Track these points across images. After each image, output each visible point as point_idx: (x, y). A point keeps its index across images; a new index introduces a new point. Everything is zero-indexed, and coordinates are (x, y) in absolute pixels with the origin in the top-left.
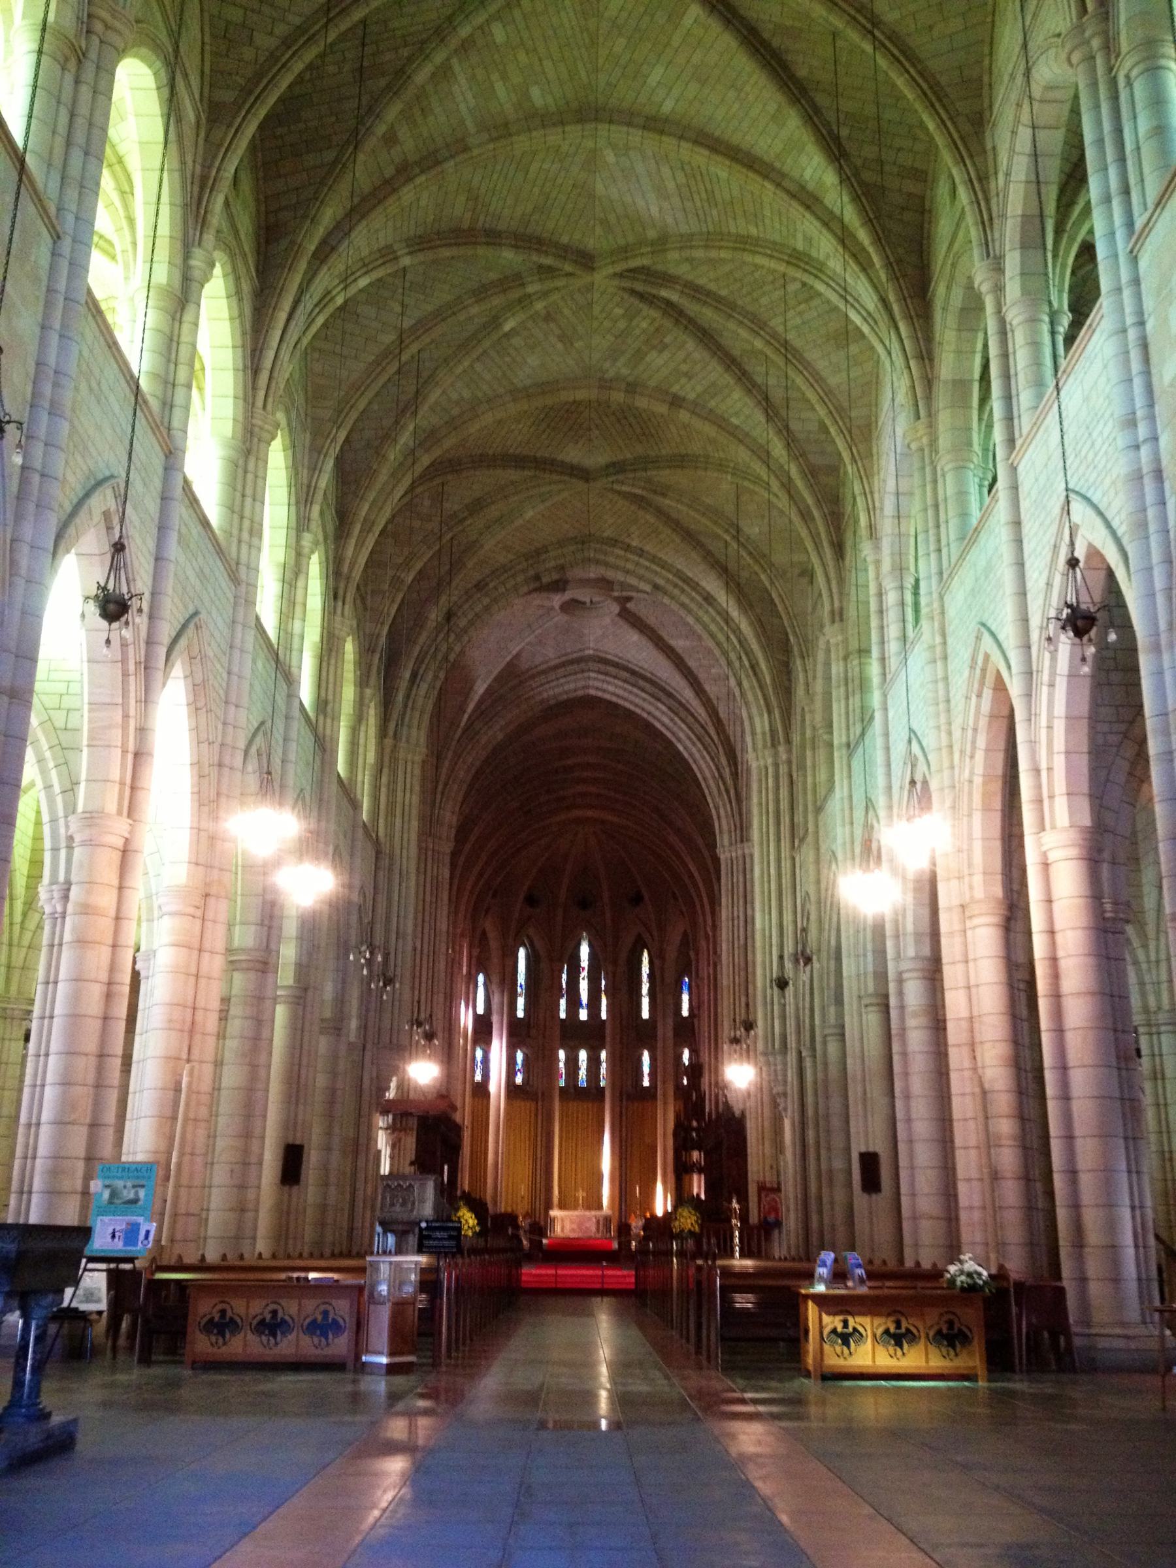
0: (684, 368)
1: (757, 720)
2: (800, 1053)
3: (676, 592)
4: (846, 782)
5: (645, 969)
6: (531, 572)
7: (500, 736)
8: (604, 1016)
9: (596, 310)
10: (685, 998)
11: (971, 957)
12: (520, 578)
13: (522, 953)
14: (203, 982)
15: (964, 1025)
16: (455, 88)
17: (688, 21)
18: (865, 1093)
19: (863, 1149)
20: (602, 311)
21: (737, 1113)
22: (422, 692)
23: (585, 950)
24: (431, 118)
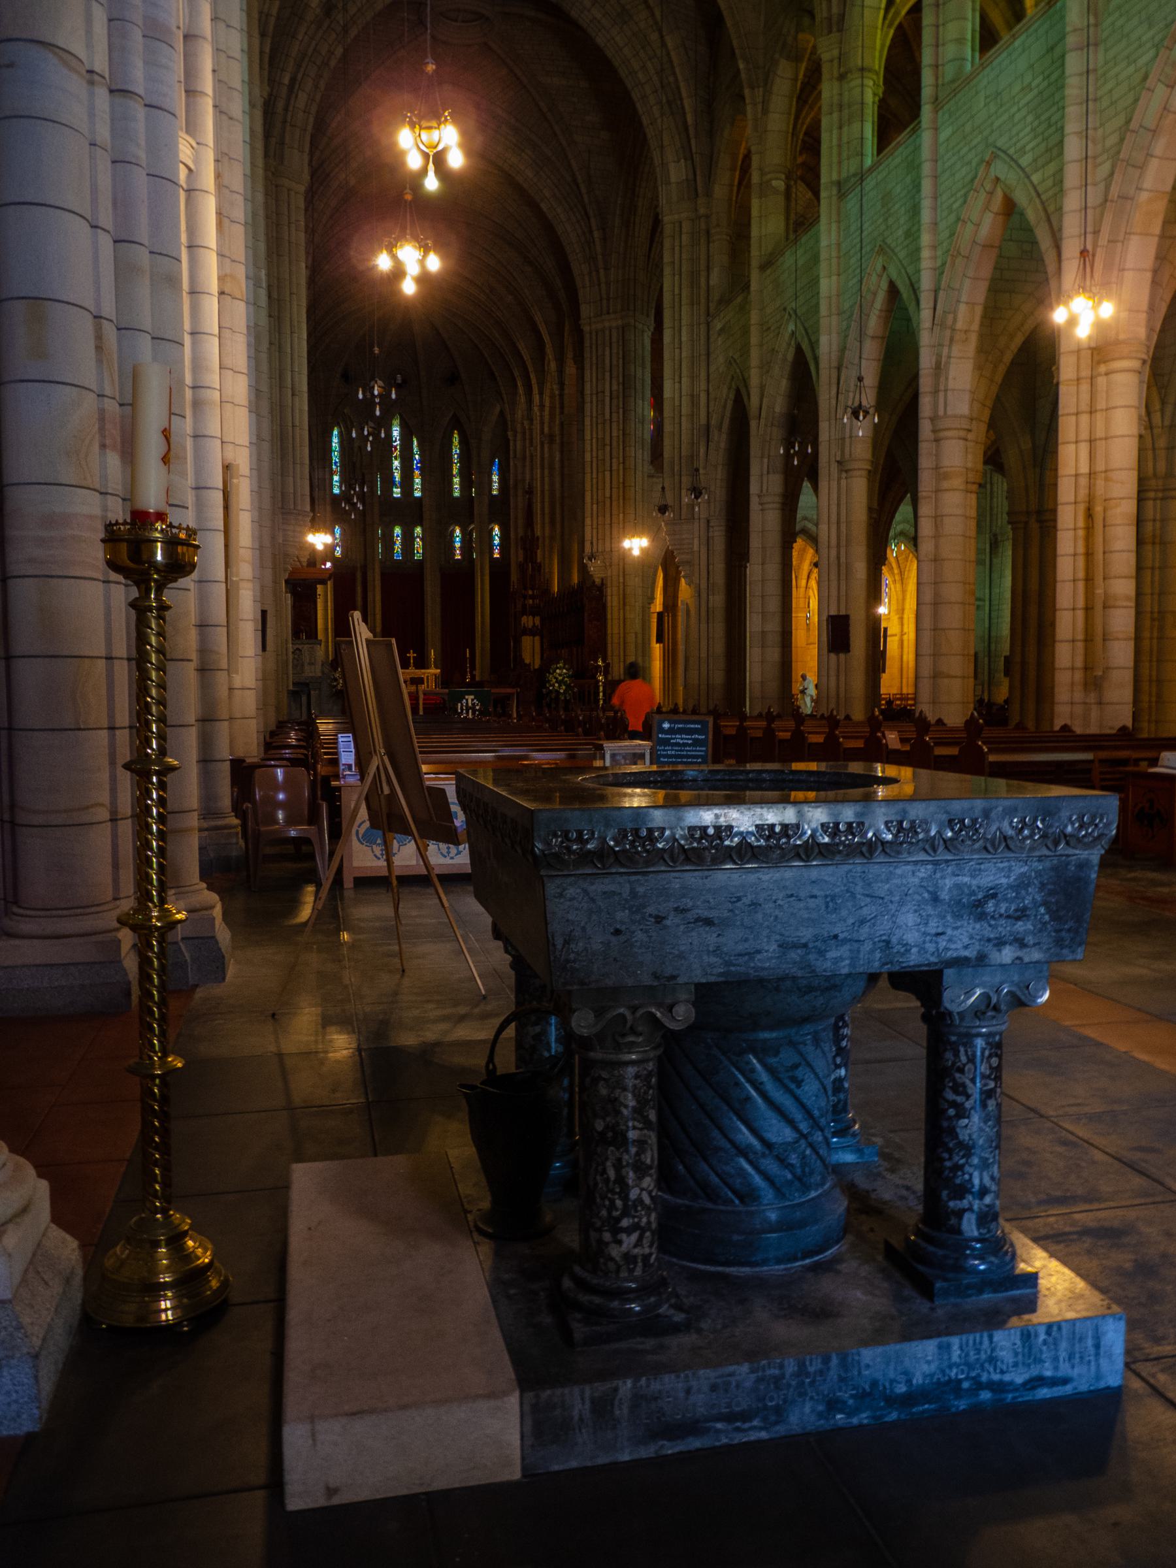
1: (672, 168)
2: (708, 521)
4: (834, 226)
5: (456, 451)
8: (418, 494)
10: (495, 478)
11: (1101, 404)
13: (335, 432)
14: (228, 406)
15: (1083, 481)
18: (838, 558)
19: (833, 612)
21: (598, 581)
23: (396, 432)
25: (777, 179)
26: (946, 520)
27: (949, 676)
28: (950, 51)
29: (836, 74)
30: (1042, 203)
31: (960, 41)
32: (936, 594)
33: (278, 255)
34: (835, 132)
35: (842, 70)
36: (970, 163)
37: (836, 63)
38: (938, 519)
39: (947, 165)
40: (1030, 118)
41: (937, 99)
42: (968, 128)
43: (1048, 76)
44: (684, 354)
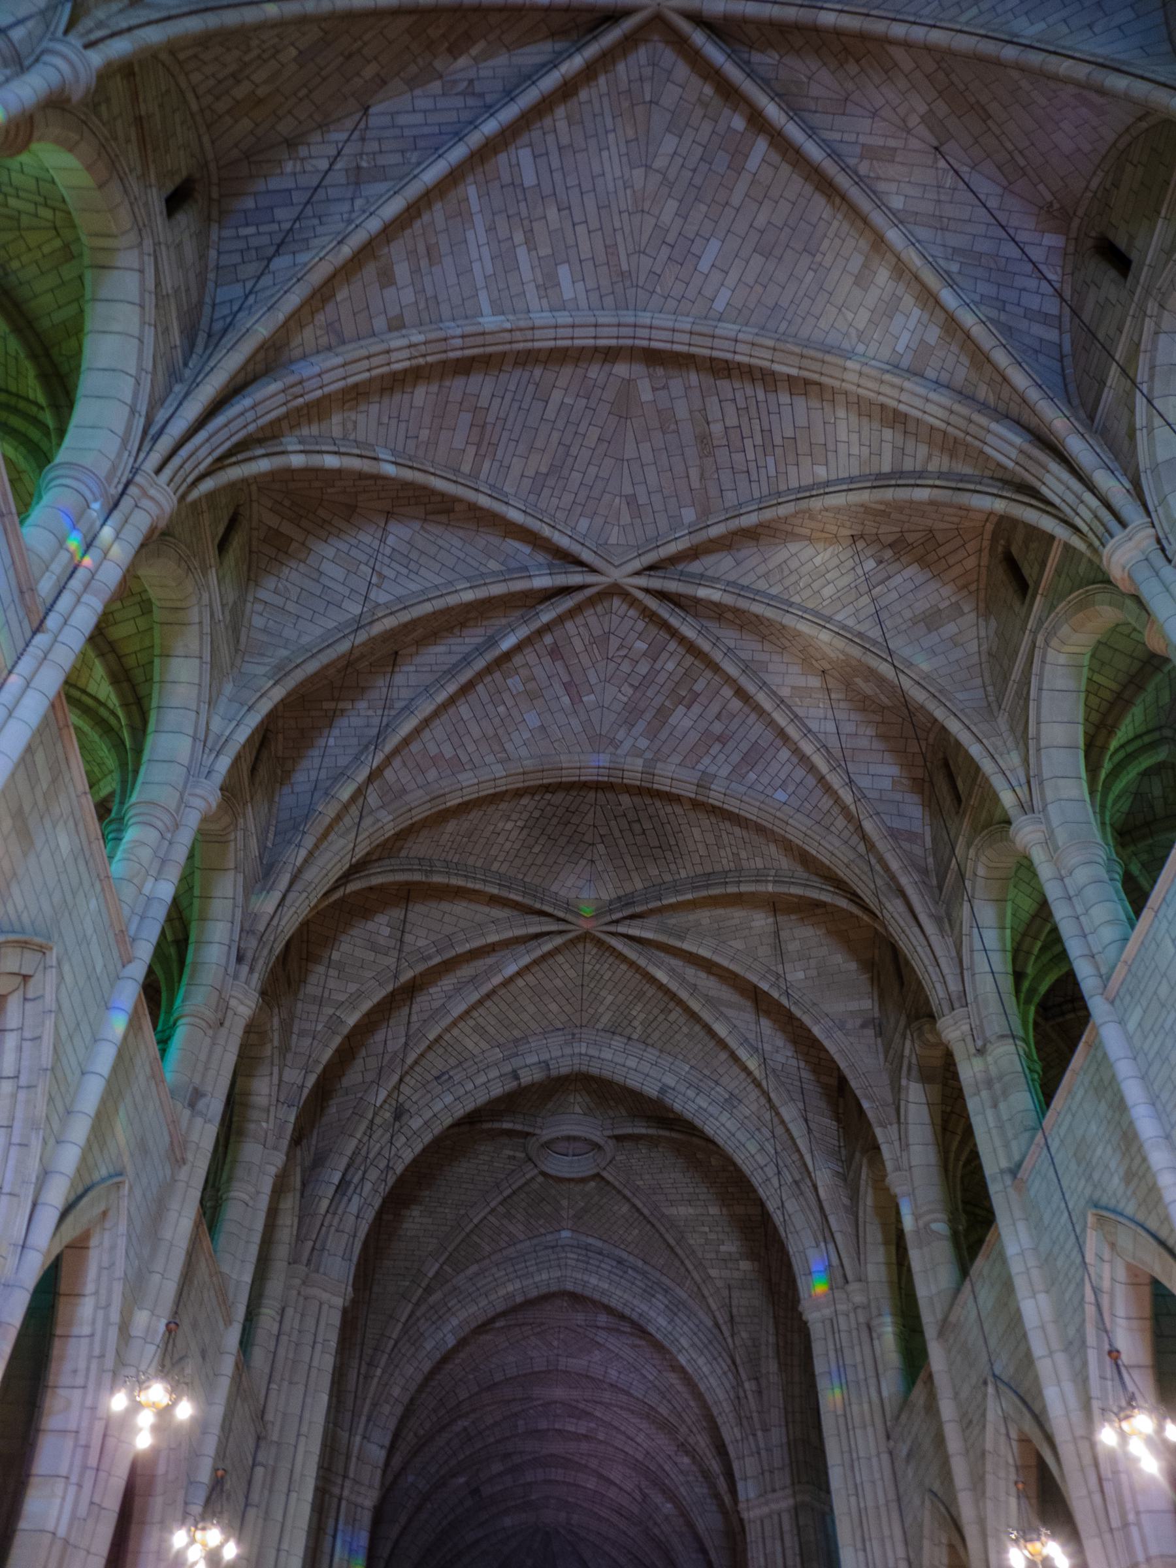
0: (717, 728)
3: (691, 1093)
4: (1021, 1226)
6: (507, 1069)
7: (451, 1341)
9: (614, 642)
12: (494, 1073)
16: (470, 235)
17: (753, 163)
20: (621, 647)
22: (353, 1208)
24: (436, 269)
25: (935, 1221)
29: (973, 1051)
33: (291, 1383)
34: (990, 1113)
35: (980, 1043)
37: (969, 1039)
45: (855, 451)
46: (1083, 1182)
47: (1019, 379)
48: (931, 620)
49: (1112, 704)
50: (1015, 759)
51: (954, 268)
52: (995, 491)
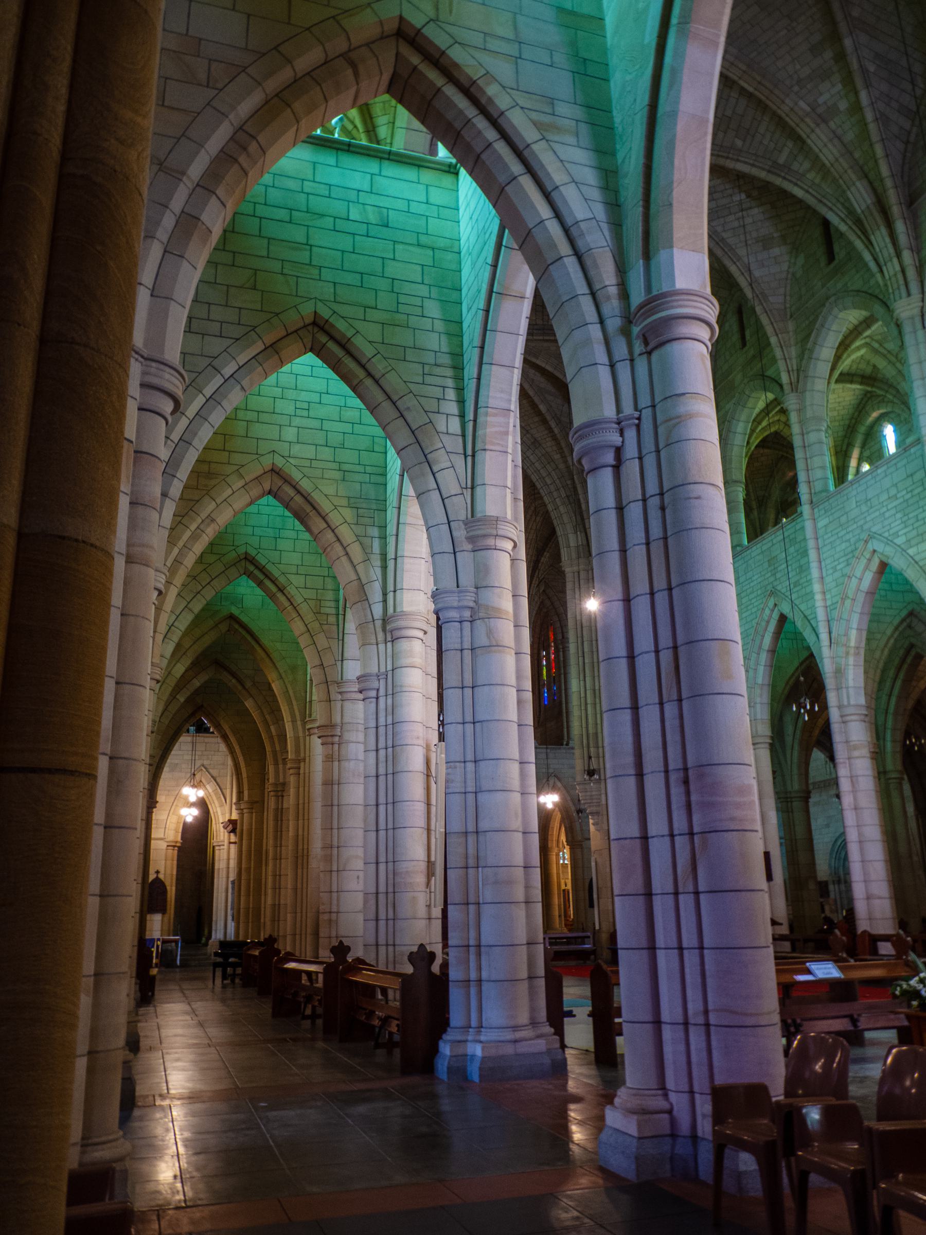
1: (572, 538)
26: (860, 779)
27: (880, 898)
28: (818, 474)
30: (921, 567)
31: (823, 468)
32: (860, 834)
36: (849, 540)
38: (853, 778)
39: (827, 542)
40: (899, 515)
41: (812, 502)
42: (844, 519)
43: (911, 491)
44: (586, 661)
45: (765, 142)
46: (769, 574)
47: (885, 171)
48: (766, 243)
49: (851, 332)
50: (793, 352)
51: (872, 68)
52: (843, 216)
